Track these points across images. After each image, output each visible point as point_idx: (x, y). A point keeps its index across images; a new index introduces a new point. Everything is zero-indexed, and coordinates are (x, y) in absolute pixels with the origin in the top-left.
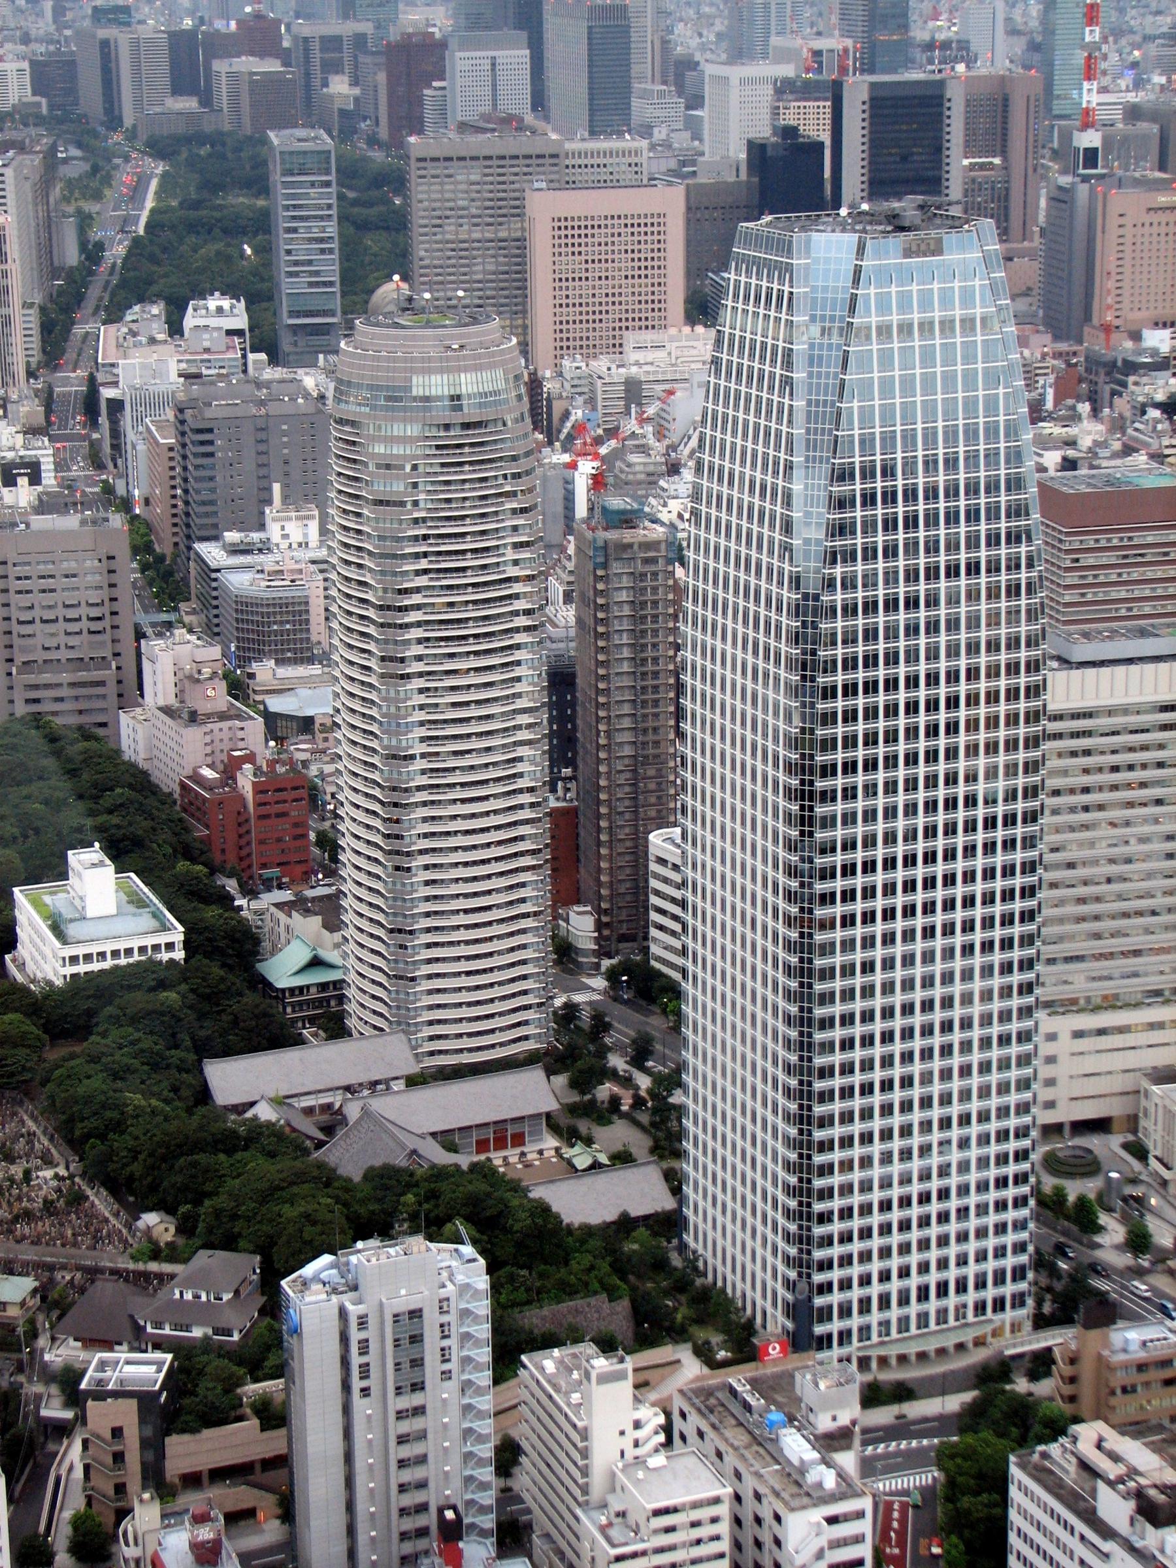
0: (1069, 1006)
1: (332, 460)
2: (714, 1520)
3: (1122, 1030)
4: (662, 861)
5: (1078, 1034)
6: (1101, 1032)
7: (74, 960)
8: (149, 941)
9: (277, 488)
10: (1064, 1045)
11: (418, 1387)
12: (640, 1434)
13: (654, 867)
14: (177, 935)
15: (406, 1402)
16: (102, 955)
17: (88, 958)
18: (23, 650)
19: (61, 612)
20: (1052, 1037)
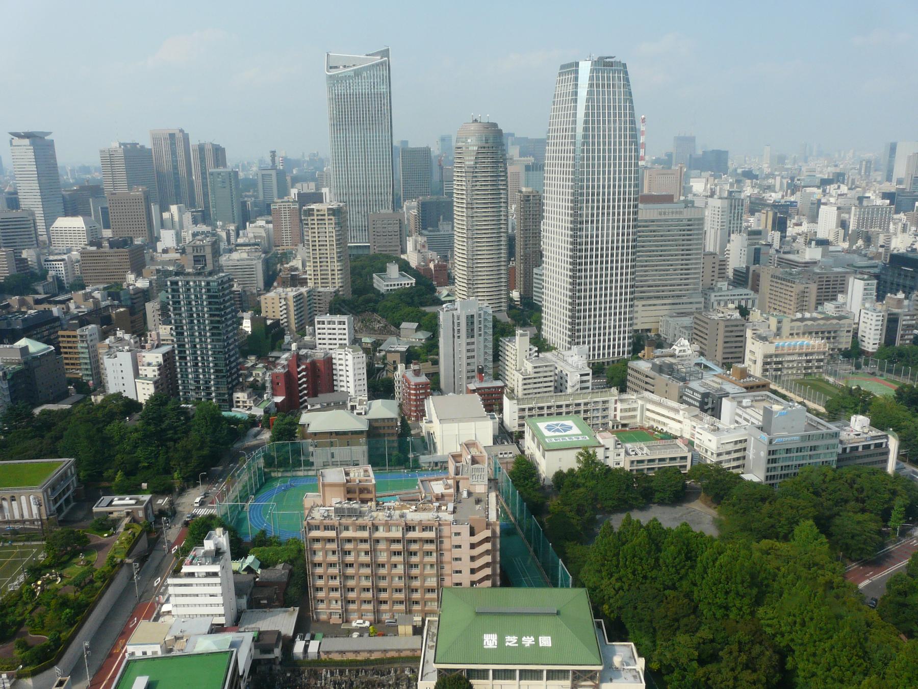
0: (642, 298)
1: (456, 241)
2: (551, 371)
3: (654, 305)
4: (536, 274)
5: (643, 306)
6: (650, 305)
7: (387, 285)
8: (406, 282)
9: (441, 217)
10: (640, 306)
11: (473, 337)
12: (531, 352)
13: (535, 276)
14: (413, 281)
15: (469, 340)
16: (394, 285)
17: (391, 285)
18: (378, 243)
19: (387, 233)
20: (637, 306)
